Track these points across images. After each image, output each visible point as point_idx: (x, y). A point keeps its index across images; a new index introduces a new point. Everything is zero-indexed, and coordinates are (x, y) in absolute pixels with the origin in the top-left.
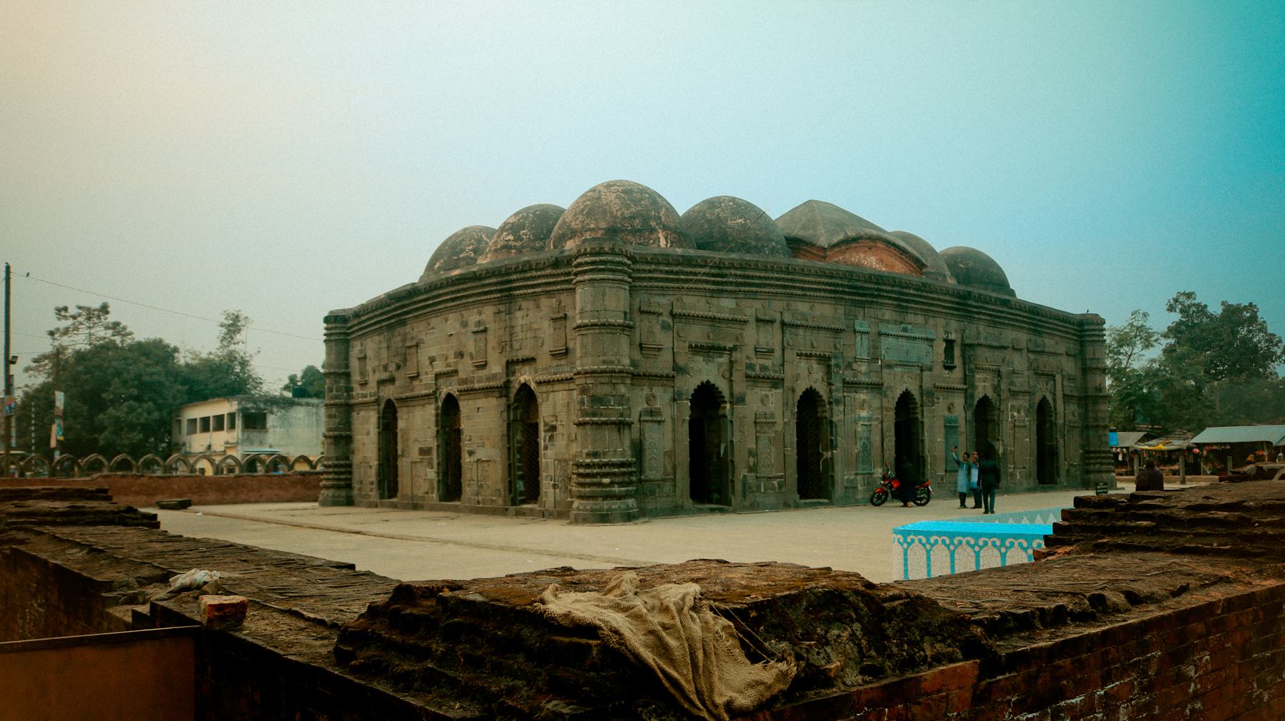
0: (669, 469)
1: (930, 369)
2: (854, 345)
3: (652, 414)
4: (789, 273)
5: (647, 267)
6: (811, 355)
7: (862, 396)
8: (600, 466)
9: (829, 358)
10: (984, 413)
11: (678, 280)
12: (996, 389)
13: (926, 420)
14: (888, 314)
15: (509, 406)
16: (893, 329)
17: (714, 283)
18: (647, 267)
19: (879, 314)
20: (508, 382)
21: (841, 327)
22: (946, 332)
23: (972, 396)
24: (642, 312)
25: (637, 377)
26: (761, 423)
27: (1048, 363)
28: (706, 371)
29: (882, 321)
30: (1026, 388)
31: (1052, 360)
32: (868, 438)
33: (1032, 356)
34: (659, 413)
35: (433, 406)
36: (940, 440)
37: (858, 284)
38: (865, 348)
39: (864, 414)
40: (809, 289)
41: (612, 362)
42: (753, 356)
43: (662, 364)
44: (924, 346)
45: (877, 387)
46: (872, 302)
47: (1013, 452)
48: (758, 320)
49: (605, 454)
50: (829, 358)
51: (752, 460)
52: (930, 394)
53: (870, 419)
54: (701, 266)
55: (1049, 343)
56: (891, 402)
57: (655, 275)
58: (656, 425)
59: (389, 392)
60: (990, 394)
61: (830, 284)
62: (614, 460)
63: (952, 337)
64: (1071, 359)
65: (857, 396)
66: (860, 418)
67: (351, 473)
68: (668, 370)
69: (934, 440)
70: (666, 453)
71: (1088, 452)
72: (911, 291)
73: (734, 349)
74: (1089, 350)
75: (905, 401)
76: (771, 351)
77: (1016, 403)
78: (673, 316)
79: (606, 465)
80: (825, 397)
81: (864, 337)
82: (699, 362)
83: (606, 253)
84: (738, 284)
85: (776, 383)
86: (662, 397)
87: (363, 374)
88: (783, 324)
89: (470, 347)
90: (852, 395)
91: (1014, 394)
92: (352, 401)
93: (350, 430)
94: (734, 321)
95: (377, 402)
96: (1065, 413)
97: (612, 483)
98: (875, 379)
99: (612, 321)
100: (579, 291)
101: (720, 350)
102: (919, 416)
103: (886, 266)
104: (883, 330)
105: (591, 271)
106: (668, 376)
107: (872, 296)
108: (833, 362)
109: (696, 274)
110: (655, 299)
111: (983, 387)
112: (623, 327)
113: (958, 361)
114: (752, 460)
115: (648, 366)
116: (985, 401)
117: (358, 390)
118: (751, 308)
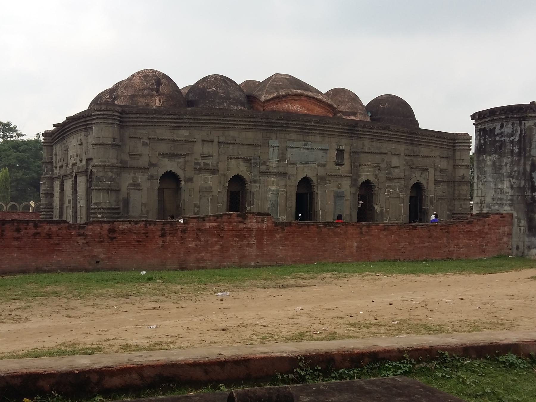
0: (144, 212)
1: (324, 165)
2: (268, 153)
3: (136, 186)
4: (224, 117)
5: (134, 116)
6: (238, 158)
7: (273, 179)
8: (99, 209)
9: (251, 159)
11: (152, 122)
12: (376, 176)
13: (319, 193)
14: (294, 136)
15: (87, 180)
16: (296, 144)
17: (175, 123)
18: (134, 116)
19: (288, 137)
20: (87, 169)
21: (259, 143)
23: (356, 180)
24: (130, 137)
25: (124, 167)
26: (205, 191)
27: (418, 162)
28: (169, 165)
29: (289, 140)
30: (402, 175)
32: (277, 201)
34: (139, 185)
35: (71, 180)
36: (330, 203)
37: (273, 121)
39: (273, 188)
40: (237, 125)
41: (105, 161)
42: (198, 157)
43: (143, 162)
44: (321, 153)
45: (283, 175)
46: (282, 130)
47: (386, 211)
48: (203, 141)
49: (100, 203)
50: (251, 159)
51: (196, 210)
52: (322, 179)
53: (277, 190)
54: (168, 115)
55: (424, 151)
56: (294, 182)
57: (138, 120)
58: (137, 191)
59: (62, 173)
60: (371, 179)
61: (253, 122)
62: (104, 206)
64: (443, 159)
65: (269, 179)
66: (270, 190)
67: (53, 212)
68: (146, 165)
70: (142, 205)
71: (453, 214)
72: (313, 124)
73: (188, 154)
74: (458, 154)
75: (306, 182)
76: (210, 156)
77: (391, 184)
78: (150, 139)
79: (100, 208)
80: (247, 179)
81: (277, 148)
82: (166, 161)
83: (103, 110)
84: (190, 123)
85: (214, 171)
86: (141, 178)
87: (56, 162)
88: (219, 142)
89: (79, 153)
90: (265, 178)
91: (390, 179)
92: (54, 176)
93: (53, 190)
94: (185, 141)
95: (59, 176)
96: (432, 190)
97: (102, 217)
98: (282, 170)
99: (105, 142)
100: (95, 128)
101: (179, 156)
102: (315, 190)
103: (308, 109)
104: (288, 145)
105: (97, 118)
106: (144, 168)
107: (282, 127)
108: (253, 161)
109: (163, 118)
110: (139, 131)
111: (365, 175)
112: (112, 145)
114: (196, 210)
115: (132, 163)
116: (367, 184)
117: (56, 171)
118: (199, 135)
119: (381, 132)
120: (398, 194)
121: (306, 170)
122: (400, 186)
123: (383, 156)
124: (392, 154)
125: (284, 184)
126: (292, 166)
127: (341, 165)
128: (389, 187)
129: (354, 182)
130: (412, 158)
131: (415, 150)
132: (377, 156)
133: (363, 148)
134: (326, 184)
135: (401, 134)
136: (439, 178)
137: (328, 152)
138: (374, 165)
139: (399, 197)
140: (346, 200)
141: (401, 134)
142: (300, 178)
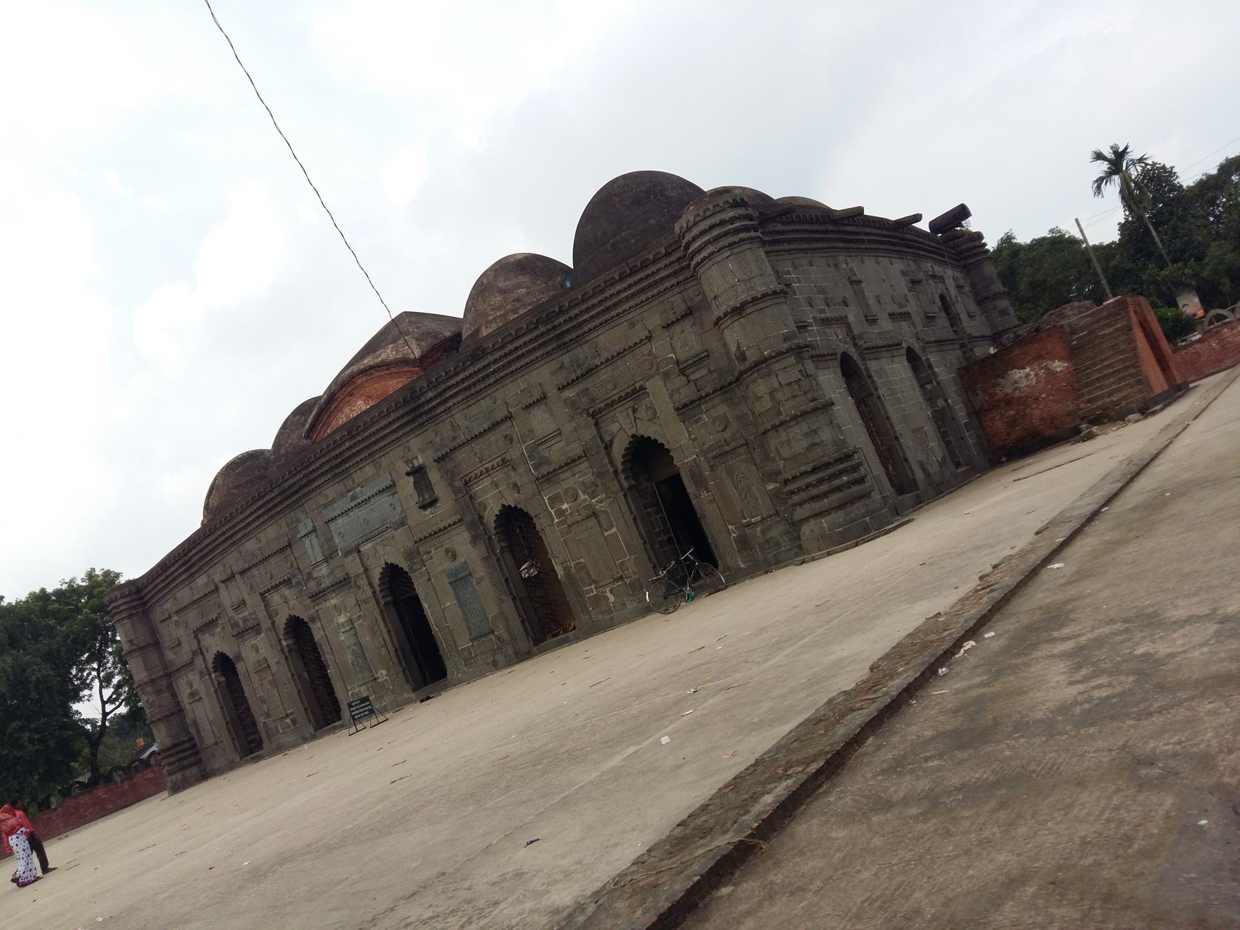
10: (516, 531)
14: (330, 492)
22: (408, 461)
29: (326, 506)
30: (576, 449)
31: (629, 362)
33: (570, 393)
36: (450, 603)
38: (316, 545)
47: (580, 567)
52: (411, 555)
53: (351, 621)
60: (511, 499)
63: (420, 460)
69: (440, 607)
81: (313, 536)
91: (547, 479)
98: (339, 575)
113: (441, 488)
119: (471, 371)
120: (590, 505)
121: (380, 548)
122: (583, 483)
123: (505, 428)
124: (528, 407)
125: (354, 601)
126: (350, 558)
127: (433, 502)
128: (555, 500)
129: (477, 526)
130: (581, 387)
131: (581, 356)
132: (492, 437)
133: (454, 438)
134: (423, 563)
135: (521, 341)
136: (688, 393)
137: (398, 488)
138: (495, 462)
139: (595, 514)
140: (479, 581)
141: (521, 341)
142: (376, 574)
